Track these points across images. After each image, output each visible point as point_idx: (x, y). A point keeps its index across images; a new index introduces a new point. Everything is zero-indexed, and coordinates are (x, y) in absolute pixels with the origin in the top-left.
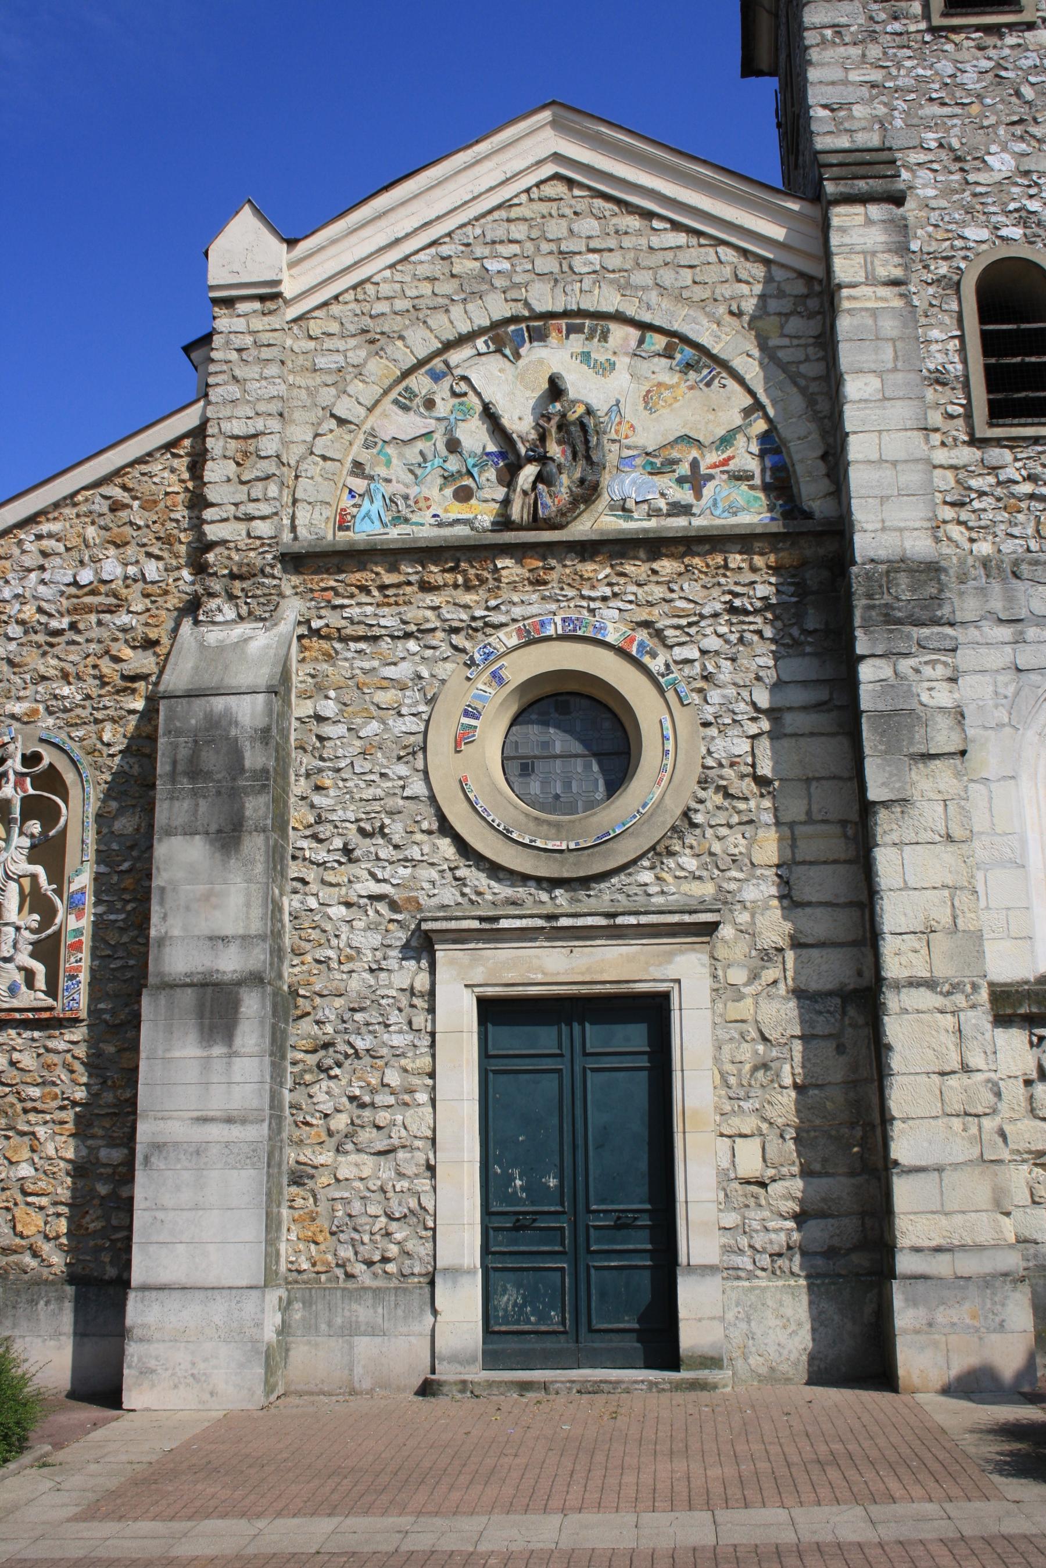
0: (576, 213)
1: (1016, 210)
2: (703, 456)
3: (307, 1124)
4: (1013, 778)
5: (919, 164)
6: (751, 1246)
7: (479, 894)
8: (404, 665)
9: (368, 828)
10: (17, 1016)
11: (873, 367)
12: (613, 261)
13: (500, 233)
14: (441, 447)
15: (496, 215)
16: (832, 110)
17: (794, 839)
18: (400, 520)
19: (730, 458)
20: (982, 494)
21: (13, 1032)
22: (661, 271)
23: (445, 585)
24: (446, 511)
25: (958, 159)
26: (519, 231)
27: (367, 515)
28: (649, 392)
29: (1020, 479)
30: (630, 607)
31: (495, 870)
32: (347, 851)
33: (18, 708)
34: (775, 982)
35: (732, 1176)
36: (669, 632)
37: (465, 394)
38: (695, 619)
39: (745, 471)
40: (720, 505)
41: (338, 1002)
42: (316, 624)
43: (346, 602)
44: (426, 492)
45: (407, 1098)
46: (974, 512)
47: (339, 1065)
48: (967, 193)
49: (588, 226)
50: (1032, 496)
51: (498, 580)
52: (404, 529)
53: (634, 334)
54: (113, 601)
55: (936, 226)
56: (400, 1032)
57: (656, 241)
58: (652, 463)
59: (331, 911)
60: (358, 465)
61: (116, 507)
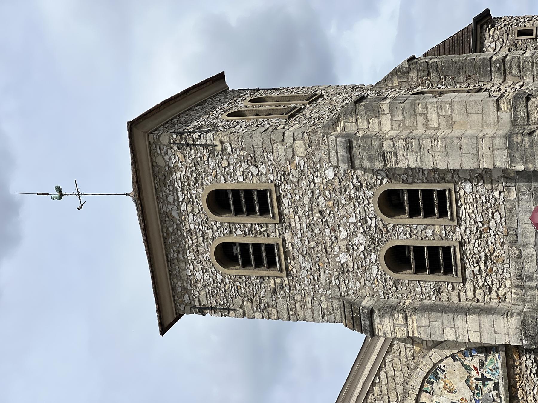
2: (473, 376)
11: (441, 329)
19: (474, 367)
20: (485, 281)
25: (343, 272)
29: (478, 267)
40: (494, 372)
46: (493, 284)
50: (486, 263)
58: (477, 393)
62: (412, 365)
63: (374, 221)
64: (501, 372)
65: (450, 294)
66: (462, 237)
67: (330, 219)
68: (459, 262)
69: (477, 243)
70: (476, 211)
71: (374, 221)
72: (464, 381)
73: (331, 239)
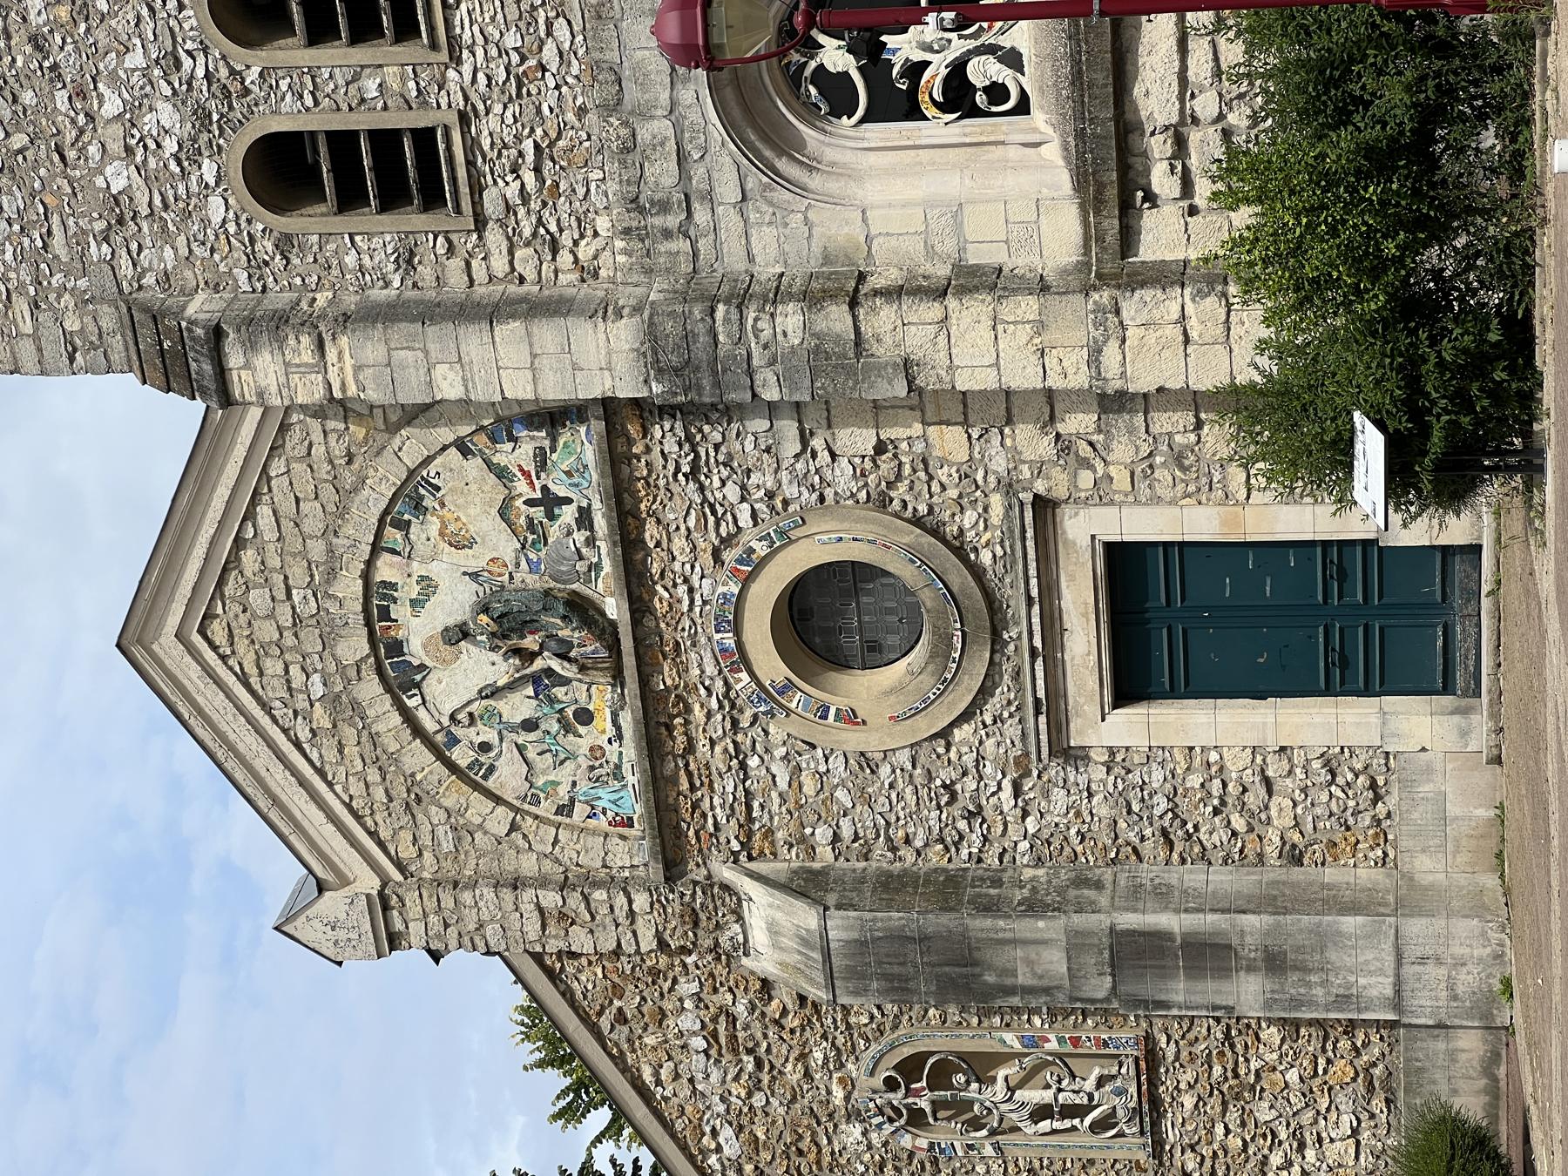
0: (244, 611)
1: (179, 164)
3: (1241, 851)
4: (864, 212)
5: (134, 265)
7: (1009, 703)
8: (774, 769)
9: (944, 800)
10: (1144, 1088)
11: (422, 371)
12: (298, 573)
13: (278, 684)
14: (532, 736)
15: (257, 687)
16: (75, 350)
17: (940, 423)
18: (617, 773)
19: (521, 469)
20: (540, 222)
21: (1162, 1089)
22: (306, 529)
23: (686, 734)
24: (604, 732)
25: (121, 221)
26: (273, 667)
27: (614, 802)
28: (451, 545)
29: (518, 182)
30: (698, 569)
31: (985, 692)
32: (970, 816)
33: (838, 1094)
34: (1091, 444)
36: (723, 532)
37: (471, 715)
38: (707, 511)
39: (535, 456)
40: (575, 480)
41: (1122, 825)
42: (735, 846)
43: (710, 821)
44: (585, 750)
45: (1214, 769)
46: (561, 231)
47: (1184, 823)
48: (164, 215)
49: (258, 599)
50: (537, 170)
51: (676, 687)
52: (626, 768)
53: (384, 560)
54: (722, 1019)
55: (212, 250)
57: (269, 534)
58: (533, 543)
59: (1031, 831)
60: (560, 810)
61: (621, 1017)
62: (348, 479)
63: (201, 60)
64: (595, 477)
65: (444, 267)
66: (466, 98)
67: (68, 61)
68: (462, 173)
69: (509, 114)
70: (500, 16)
71: (201, 60)
72: (494, 511)
73: (73, 121)
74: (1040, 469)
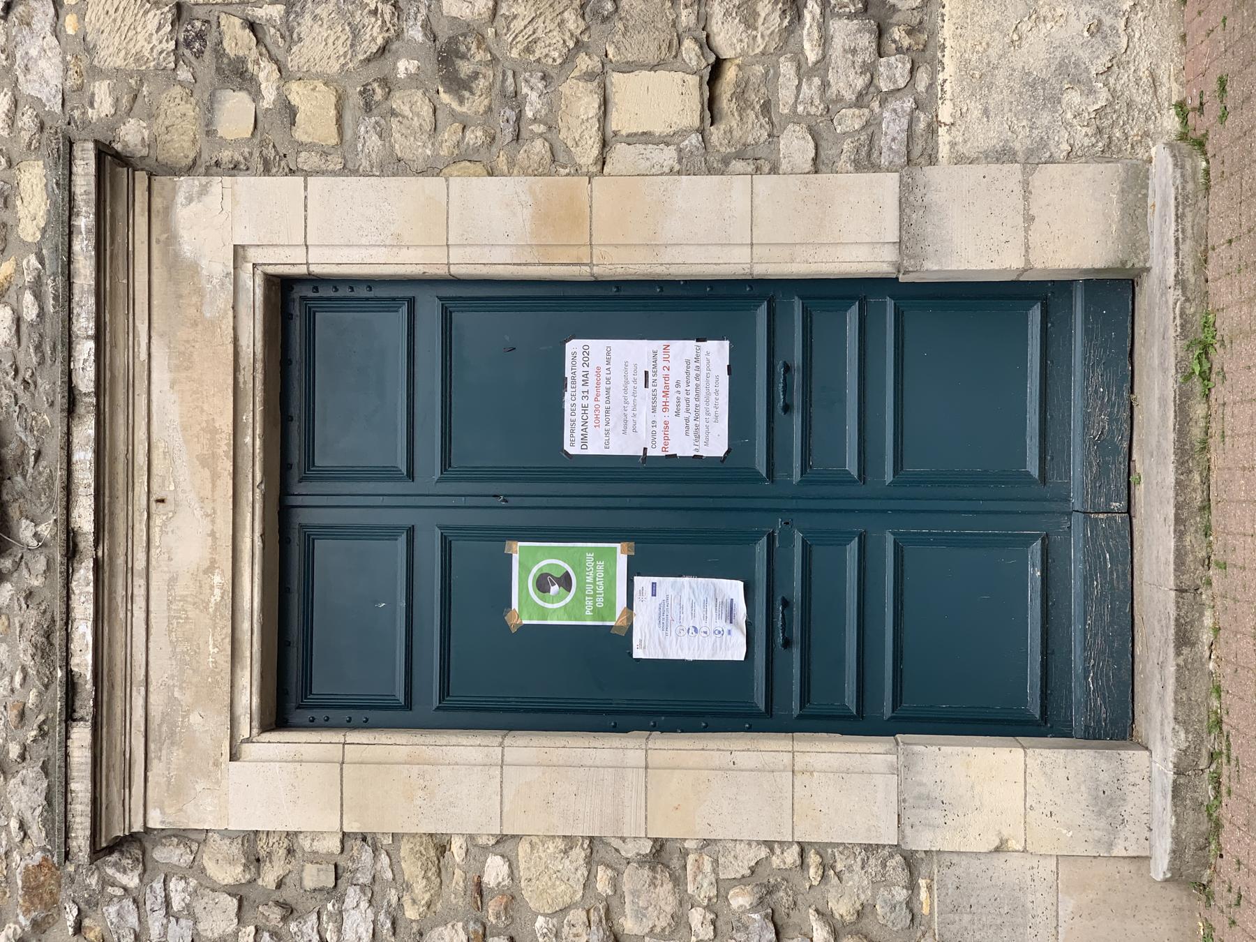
6: (860, 100)
34: (252, 26)
35: (695, 139)
56: (339, 917)
74: (135, 93)
